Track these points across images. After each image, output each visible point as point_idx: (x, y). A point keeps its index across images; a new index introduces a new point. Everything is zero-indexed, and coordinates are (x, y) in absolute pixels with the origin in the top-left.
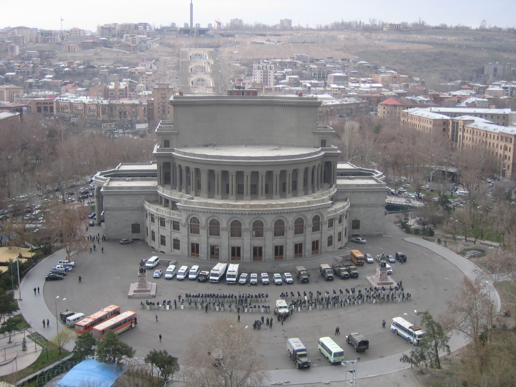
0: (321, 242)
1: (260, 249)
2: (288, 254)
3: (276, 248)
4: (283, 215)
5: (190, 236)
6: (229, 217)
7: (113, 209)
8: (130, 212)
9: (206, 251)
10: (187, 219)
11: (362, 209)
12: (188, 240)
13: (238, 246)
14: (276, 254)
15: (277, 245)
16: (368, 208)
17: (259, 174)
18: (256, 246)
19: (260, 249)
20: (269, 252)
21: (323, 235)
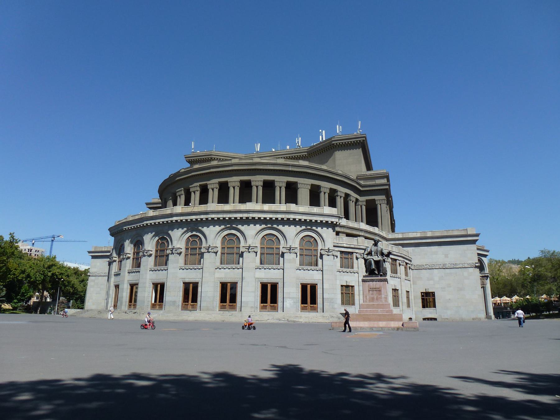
3: (224, 286)
14: (223, 300)
15: (224, 280)
18: (187, 280)
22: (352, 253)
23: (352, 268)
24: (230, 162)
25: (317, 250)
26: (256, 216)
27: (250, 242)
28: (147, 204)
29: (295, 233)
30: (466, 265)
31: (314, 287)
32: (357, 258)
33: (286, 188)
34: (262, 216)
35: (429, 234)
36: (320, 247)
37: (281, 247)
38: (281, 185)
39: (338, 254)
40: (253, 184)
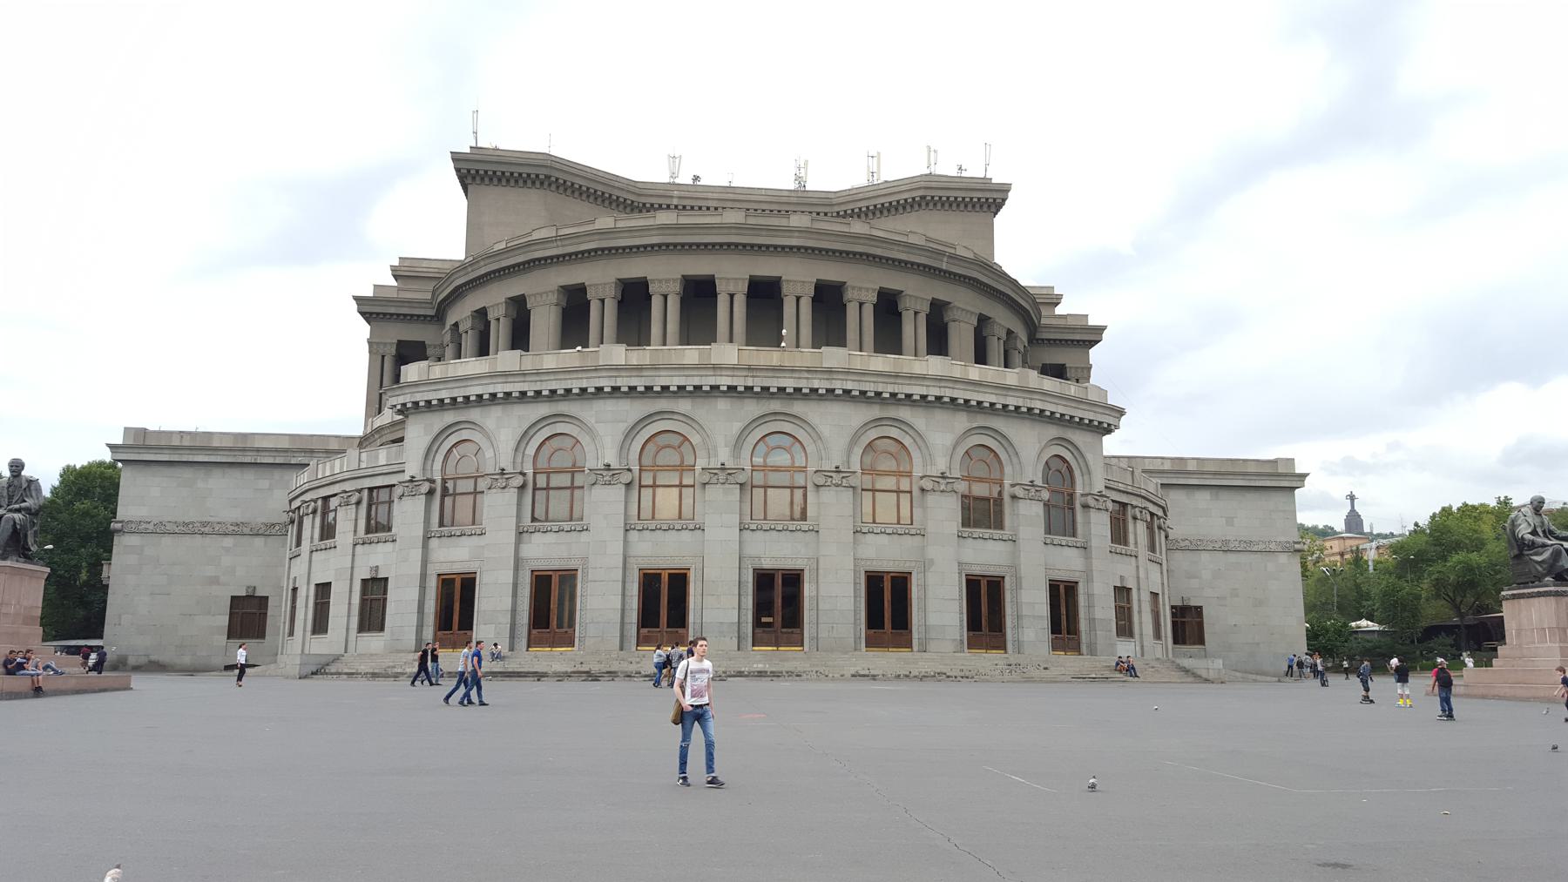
0: (1090, 596)
1: (793, 580)
2: (933, 619)
3: (874, 582)
4: (904, 413)
5: (434, 543)
6: (632, 410)
7: (159, 530)
8: (228, 542)
9: (507, 603)
10: (429, 453)
11: (1205, 556)
12: (425, 562)
13: (676, 563)
14: (874, 619)
16: (1232, 557)
17: (785, 289)
18: (767, 564)
19: (793, 580)
20: (834, 601)
21: (1096, 563)
22: (1124, 505)
23: (1126, 543)
24: (783, 222)
25: (1071, 495)
26: (961, 394)
27: (941, 465)
28: (359, 300)
29: (1037, 447)
30: (1273, 547)
31: (1071, 588)
32: (1135, 518)
33: (817, 300)
34: (974, 397)
35: (1191, 467)
36: (1079, 490)
37: (1007, 482)
38: (918, 308)
39: (1110, 505)
40: (849, 295)
